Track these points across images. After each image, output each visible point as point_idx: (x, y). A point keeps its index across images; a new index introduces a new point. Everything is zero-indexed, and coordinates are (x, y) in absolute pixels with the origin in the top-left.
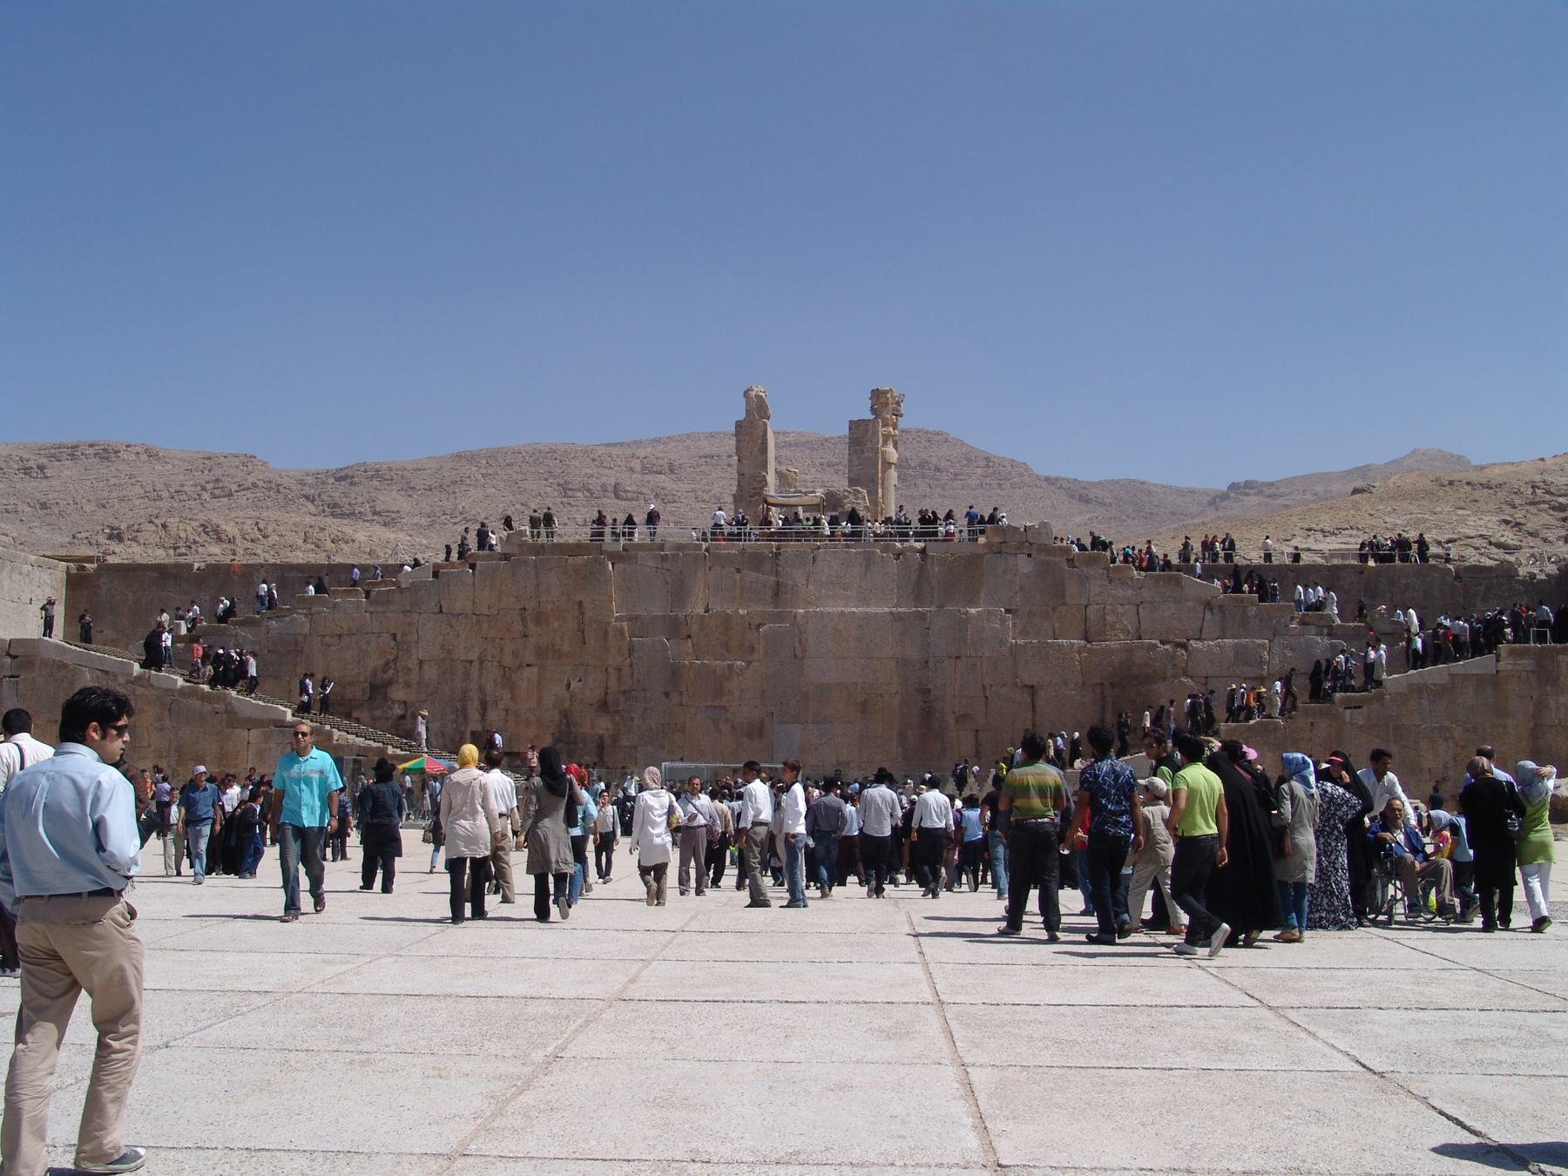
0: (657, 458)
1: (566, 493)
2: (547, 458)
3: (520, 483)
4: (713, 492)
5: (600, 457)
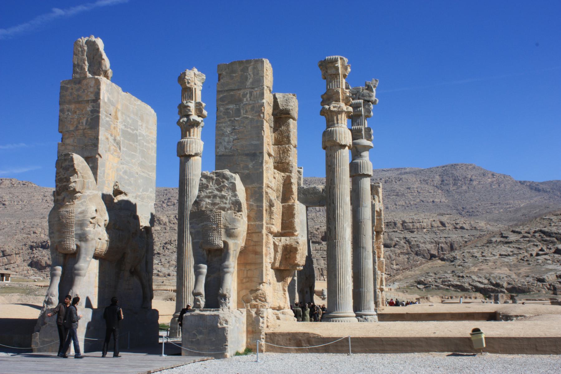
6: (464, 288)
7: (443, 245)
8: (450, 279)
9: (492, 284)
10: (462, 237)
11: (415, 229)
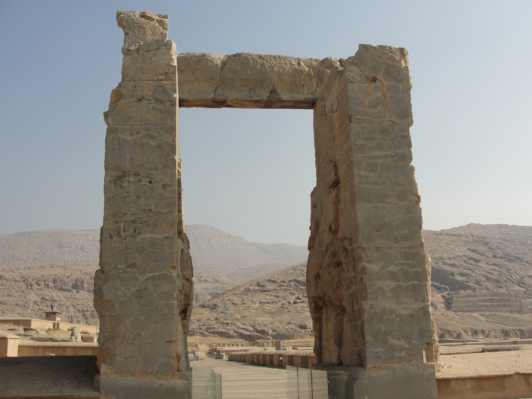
3: (42, 245)
6: (230, 335)
8: (215, 326)
9: (257, 331)
10: (206, 289)
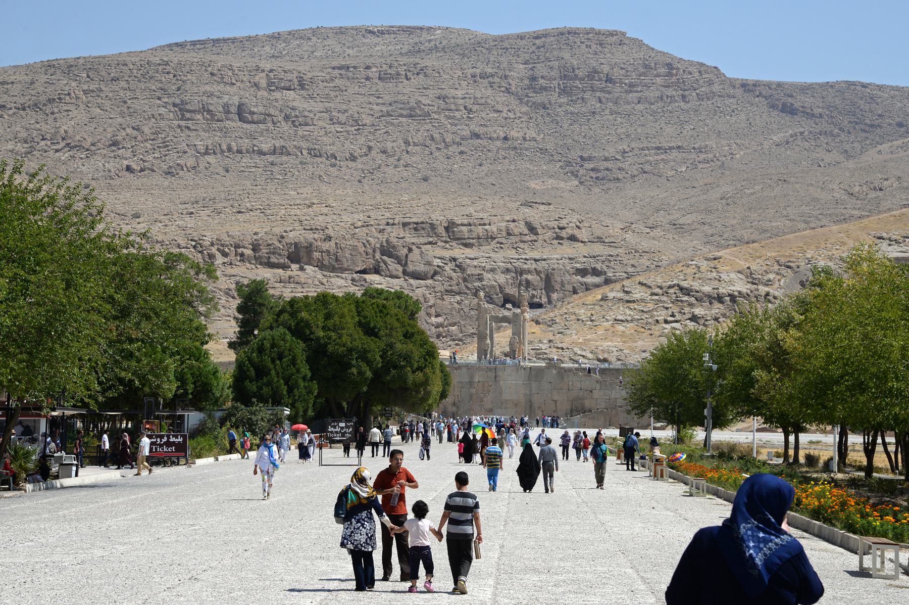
0: (285, 72)
1: (183, 115)
2: (157, 72)
3: (129, 102)
4: (350, 112)
5: (219, 70)
7: (529, 277)
10: (570, 259)
11: (473, 239)
